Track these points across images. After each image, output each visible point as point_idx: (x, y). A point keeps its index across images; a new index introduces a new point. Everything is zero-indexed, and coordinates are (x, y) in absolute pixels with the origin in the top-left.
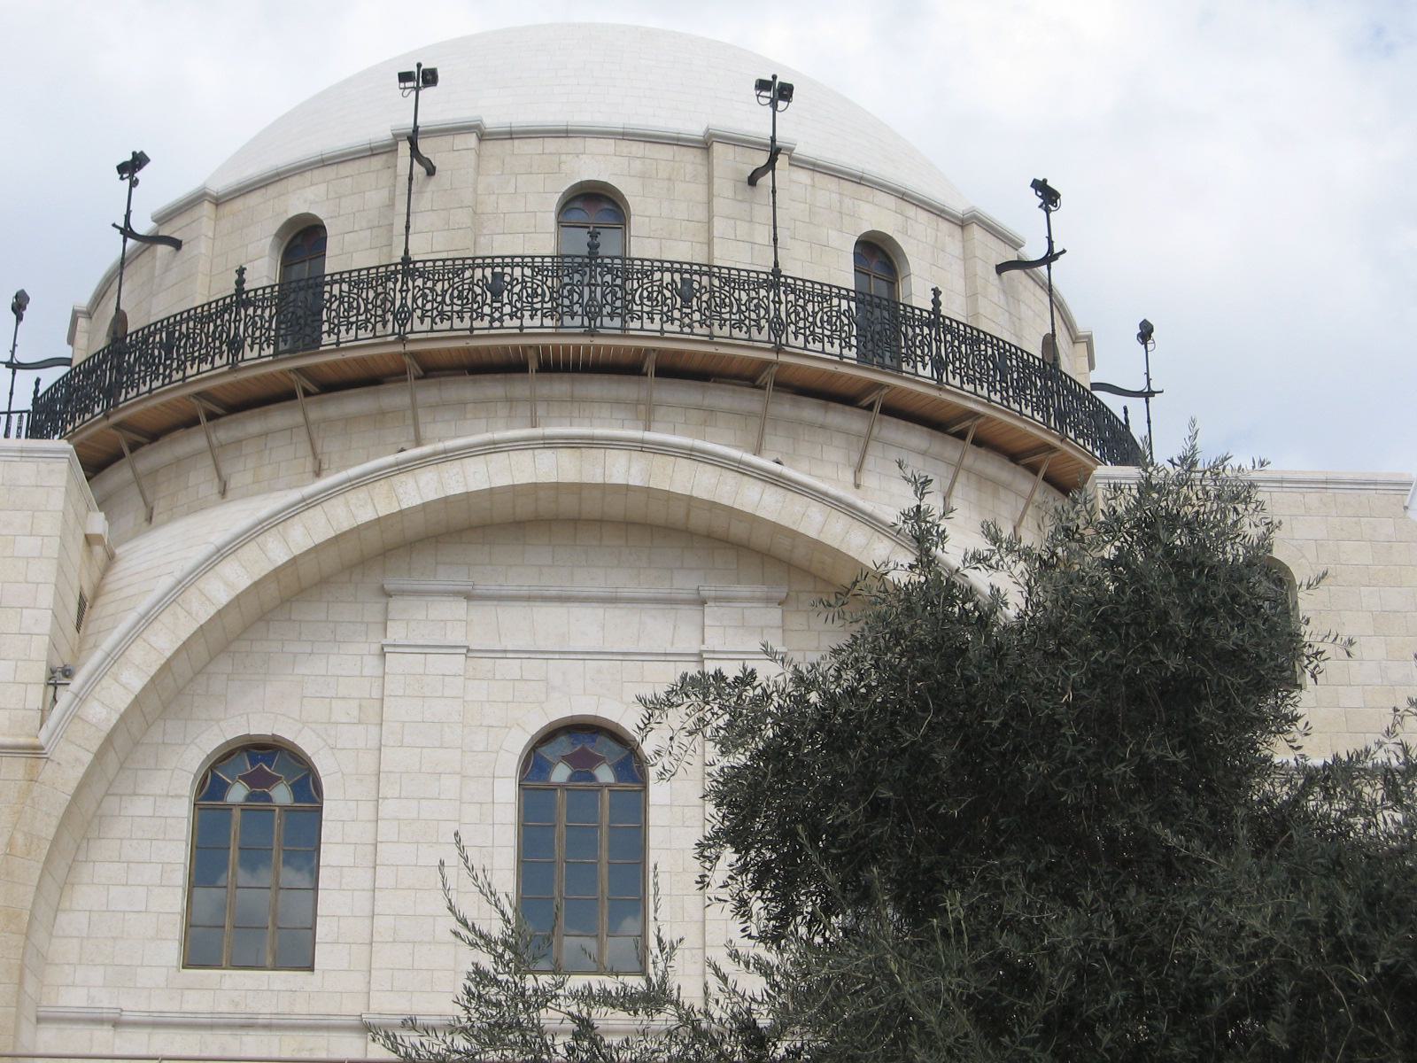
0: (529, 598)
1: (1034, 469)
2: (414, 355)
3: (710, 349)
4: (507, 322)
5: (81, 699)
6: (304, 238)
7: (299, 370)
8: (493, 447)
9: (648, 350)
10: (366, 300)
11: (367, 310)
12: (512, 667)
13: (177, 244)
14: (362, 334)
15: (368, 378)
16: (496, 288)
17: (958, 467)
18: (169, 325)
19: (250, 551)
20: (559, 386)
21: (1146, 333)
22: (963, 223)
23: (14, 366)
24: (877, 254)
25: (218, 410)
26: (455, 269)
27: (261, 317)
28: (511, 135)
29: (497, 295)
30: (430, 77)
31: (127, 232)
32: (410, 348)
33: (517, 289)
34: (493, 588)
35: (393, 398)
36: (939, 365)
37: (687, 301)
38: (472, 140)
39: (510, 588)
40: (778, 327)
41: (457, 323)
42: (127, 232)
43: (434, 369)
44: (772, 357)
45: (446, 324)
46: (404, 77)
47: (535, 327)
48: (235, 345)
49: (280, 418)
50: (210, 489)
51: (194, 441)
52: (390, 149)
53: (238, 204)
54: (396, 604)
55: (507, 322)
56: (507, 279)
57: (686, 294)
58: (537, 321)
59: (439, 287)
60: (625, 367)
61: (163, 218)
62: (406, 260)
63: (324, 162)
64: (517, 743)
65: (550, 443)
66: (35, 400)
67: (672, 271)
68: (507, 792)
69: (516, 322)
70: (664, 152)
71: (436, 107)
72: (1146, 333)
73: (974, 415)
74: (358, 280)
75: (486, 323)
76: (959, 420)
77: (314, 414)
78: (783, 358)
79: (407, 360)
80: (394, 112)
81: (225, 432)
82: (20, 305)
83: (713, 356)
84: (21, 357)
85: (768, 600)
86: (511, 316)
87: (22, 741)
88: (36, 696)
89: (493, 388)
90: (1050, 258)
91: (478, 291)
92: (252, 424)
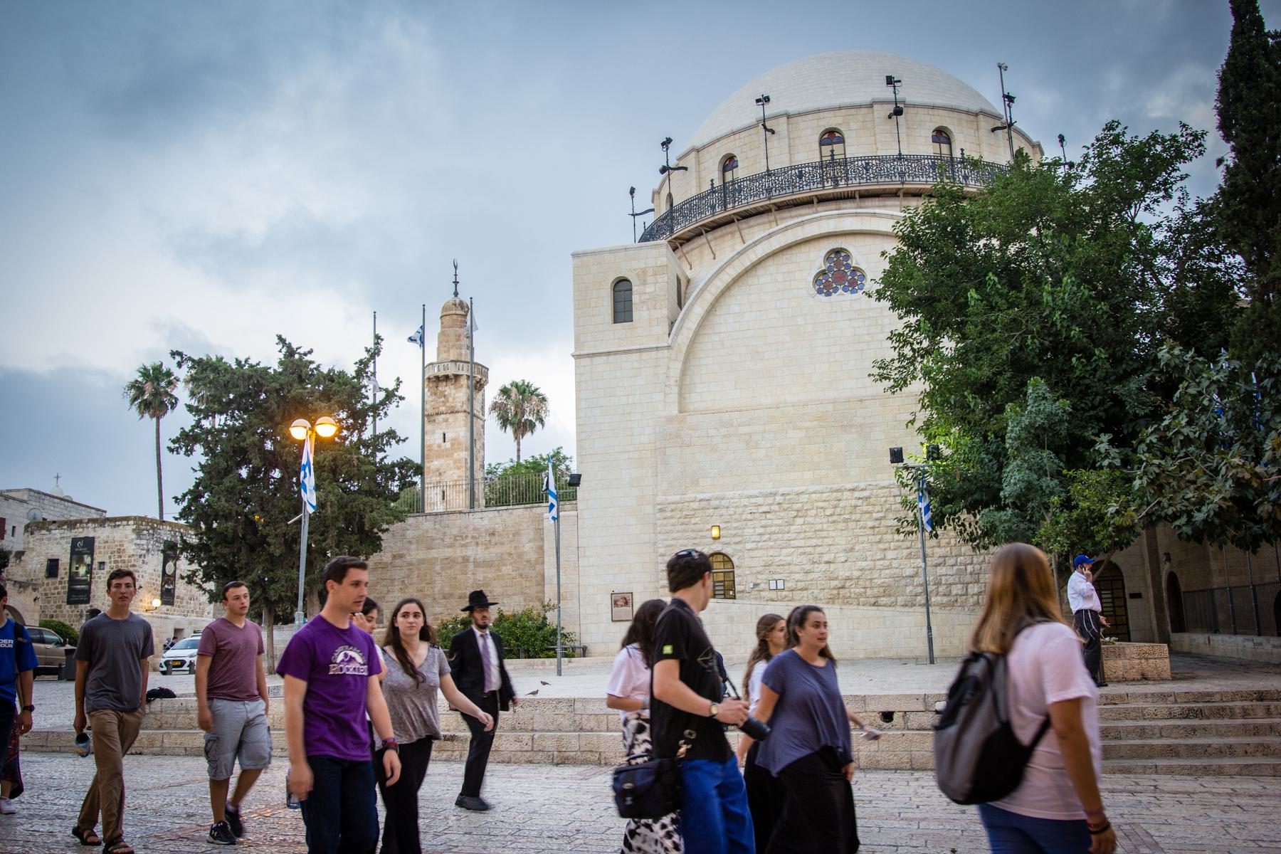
6: (729, 162)
13: (686, 169)
16: (800, 176)
18: (689, 201)
22: (976, 115)
23: (634, 215)
26: (784, 171)
28: (800, 114)
30: (767, 99)
38: (784, 119)
40: (902, 174)
46: (758, 101)
47: (815, 190)
48: (713, 207)
49: (728, 229)
52: (756, 126)
60: (848, 197)
71: (770, 109)
74: (752, 179)
80: (756, 112)
82: (632, 191)
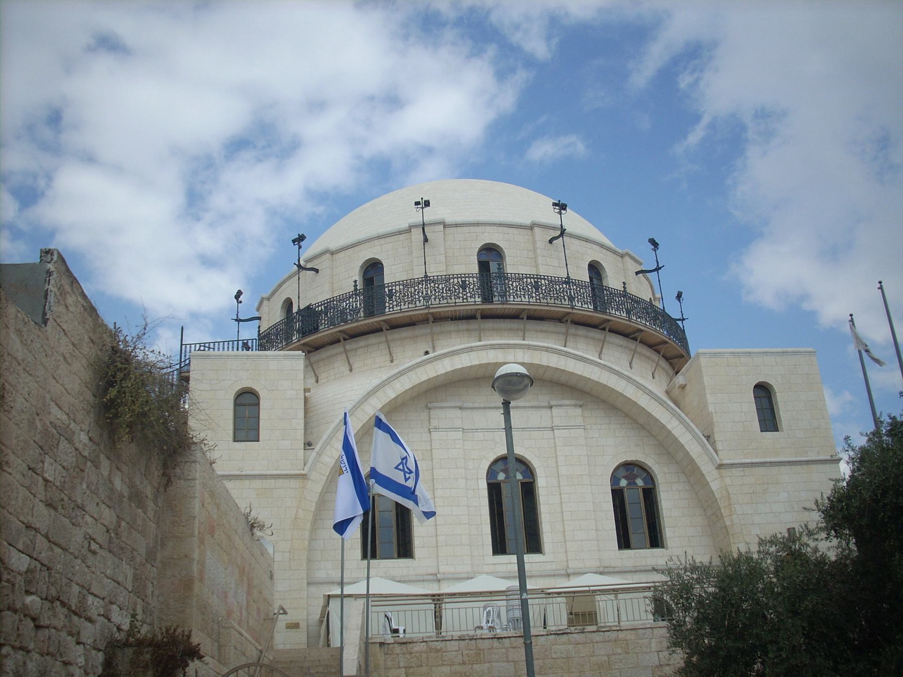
0: (484, 408)
1: (658, 352)
2: (432, 314)
3: (548, 308)
4: (469, 299)
5: (319, 454)
6: (373, 269)
7: (384, 321)
8: (471, 349)
9: (524, 309)
12: (480, 435)
13: (317, 271)
14: (410, 306)
15: (410, 323)
16: (464, 286)
17: (635, 351)
19: (380, 394)
20: (489, 324)
21: (679, 296)
23: (238, 320)
24: (595, 269)
25: (347, 337)
26: (447, 279)
28: (456, 225)
29: (464, 289)
30: (427, 204)
31: (299, 266)
32: (431, 311)
34: (470, 405)
35: (419, 330)
36: (628, 312)
37: (537, 289)
39: (477, 405)
40: (571, 299)
41: (449, 301)
42: (299, 266)
43: (438, 319)
44: (570, 311)
45: (445, 301)
46: (417, 203)
49: (372, 339)
50: (346, 368)
51: (338, 348)
53: (342, 254)
54: (434, 413)
55: (469, 299)
57: (537, 287)
60: (515, 316)
61: (307, 261)
62: (426, 276)
63: (379, 237)
64: (486, 465)
65: (493, 347)
66: (259, 335)
67: (530, 278)
68: (483, 485)
69: (473, 300)
70: (515, 231)
71: (430, 215)
72: (679, 296)
73: (641, 331)
75: (461, 300)
76: (634, 333)
77: (389, 338)
78: (574, 311)
79: (430, 316)
81: (350, 345)
83: (550, 311)
84: (241, 317)
85: (575, 405)
86: (471, 297)
87: (298, 472)
88: (301, 453)
89: (463, 325)
90: (657, 269)
92: (362, 342)
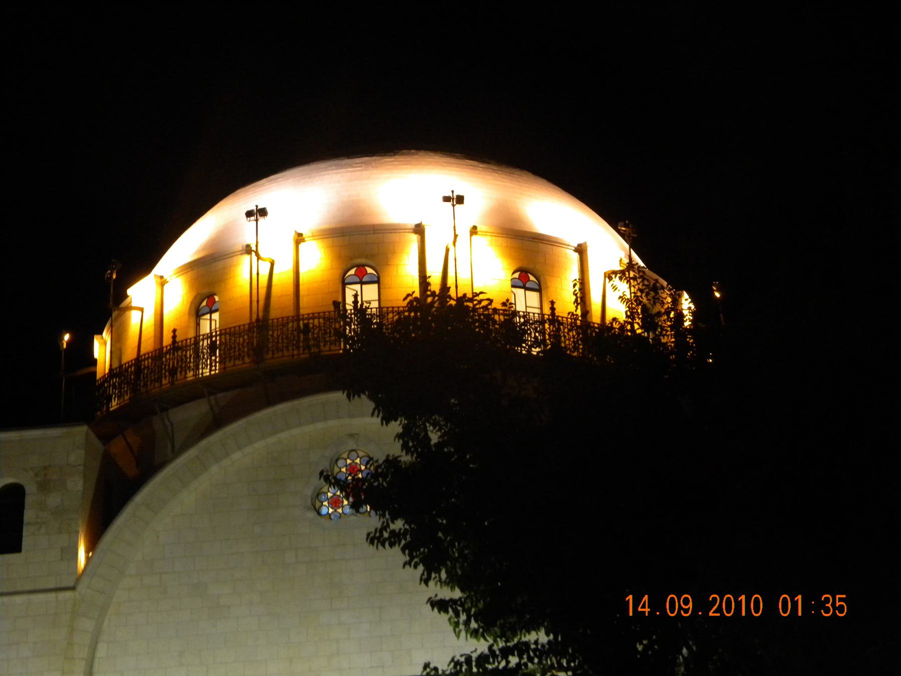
10: (239, 344)
11: (239, 349)
14: (237, 362)
27: (186, 356)
33: (316, 331)
41: (286, 353)
45: (280, 354)
56: (311, 326)
58: (327, 348)
59: (275, 335)
91: (295, 333)
